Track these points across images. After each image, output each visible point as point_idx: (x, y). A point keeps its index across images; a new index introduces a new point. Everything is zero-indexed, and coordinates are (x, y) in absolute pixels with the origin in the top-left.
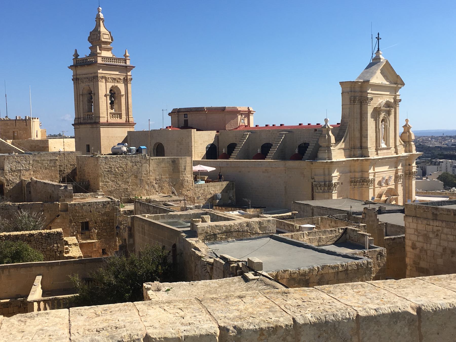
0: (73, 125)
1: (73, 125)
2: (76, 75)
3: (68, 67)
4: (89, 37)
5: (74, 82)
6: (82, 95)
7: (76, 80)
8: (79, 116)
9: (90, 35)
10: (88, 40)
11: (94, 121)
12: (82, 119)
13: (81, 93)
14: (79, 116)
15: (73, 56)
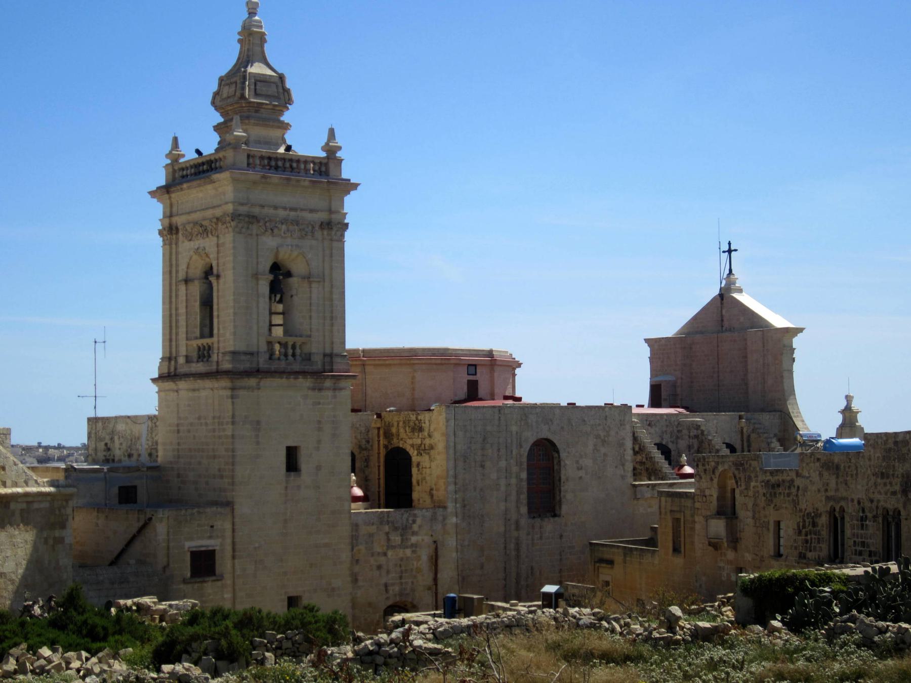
0: (154, 380)
1: (154, 380)
2: (171, 216)
3: (151, 193)
4: (216, 94)
5: (164, 240)
6: (187, 281)
7: (170, 231)
8: (174, 350)
9: (220, 85)
10: (213, 103)
11: (214, 368)
12: (181, 360)
13: (182, 275)
14: (174, 350)
15: (167, 156)
